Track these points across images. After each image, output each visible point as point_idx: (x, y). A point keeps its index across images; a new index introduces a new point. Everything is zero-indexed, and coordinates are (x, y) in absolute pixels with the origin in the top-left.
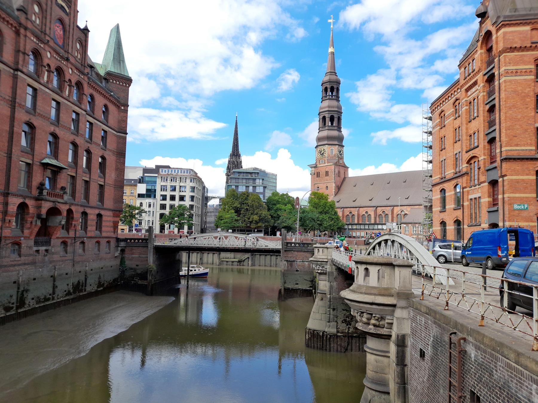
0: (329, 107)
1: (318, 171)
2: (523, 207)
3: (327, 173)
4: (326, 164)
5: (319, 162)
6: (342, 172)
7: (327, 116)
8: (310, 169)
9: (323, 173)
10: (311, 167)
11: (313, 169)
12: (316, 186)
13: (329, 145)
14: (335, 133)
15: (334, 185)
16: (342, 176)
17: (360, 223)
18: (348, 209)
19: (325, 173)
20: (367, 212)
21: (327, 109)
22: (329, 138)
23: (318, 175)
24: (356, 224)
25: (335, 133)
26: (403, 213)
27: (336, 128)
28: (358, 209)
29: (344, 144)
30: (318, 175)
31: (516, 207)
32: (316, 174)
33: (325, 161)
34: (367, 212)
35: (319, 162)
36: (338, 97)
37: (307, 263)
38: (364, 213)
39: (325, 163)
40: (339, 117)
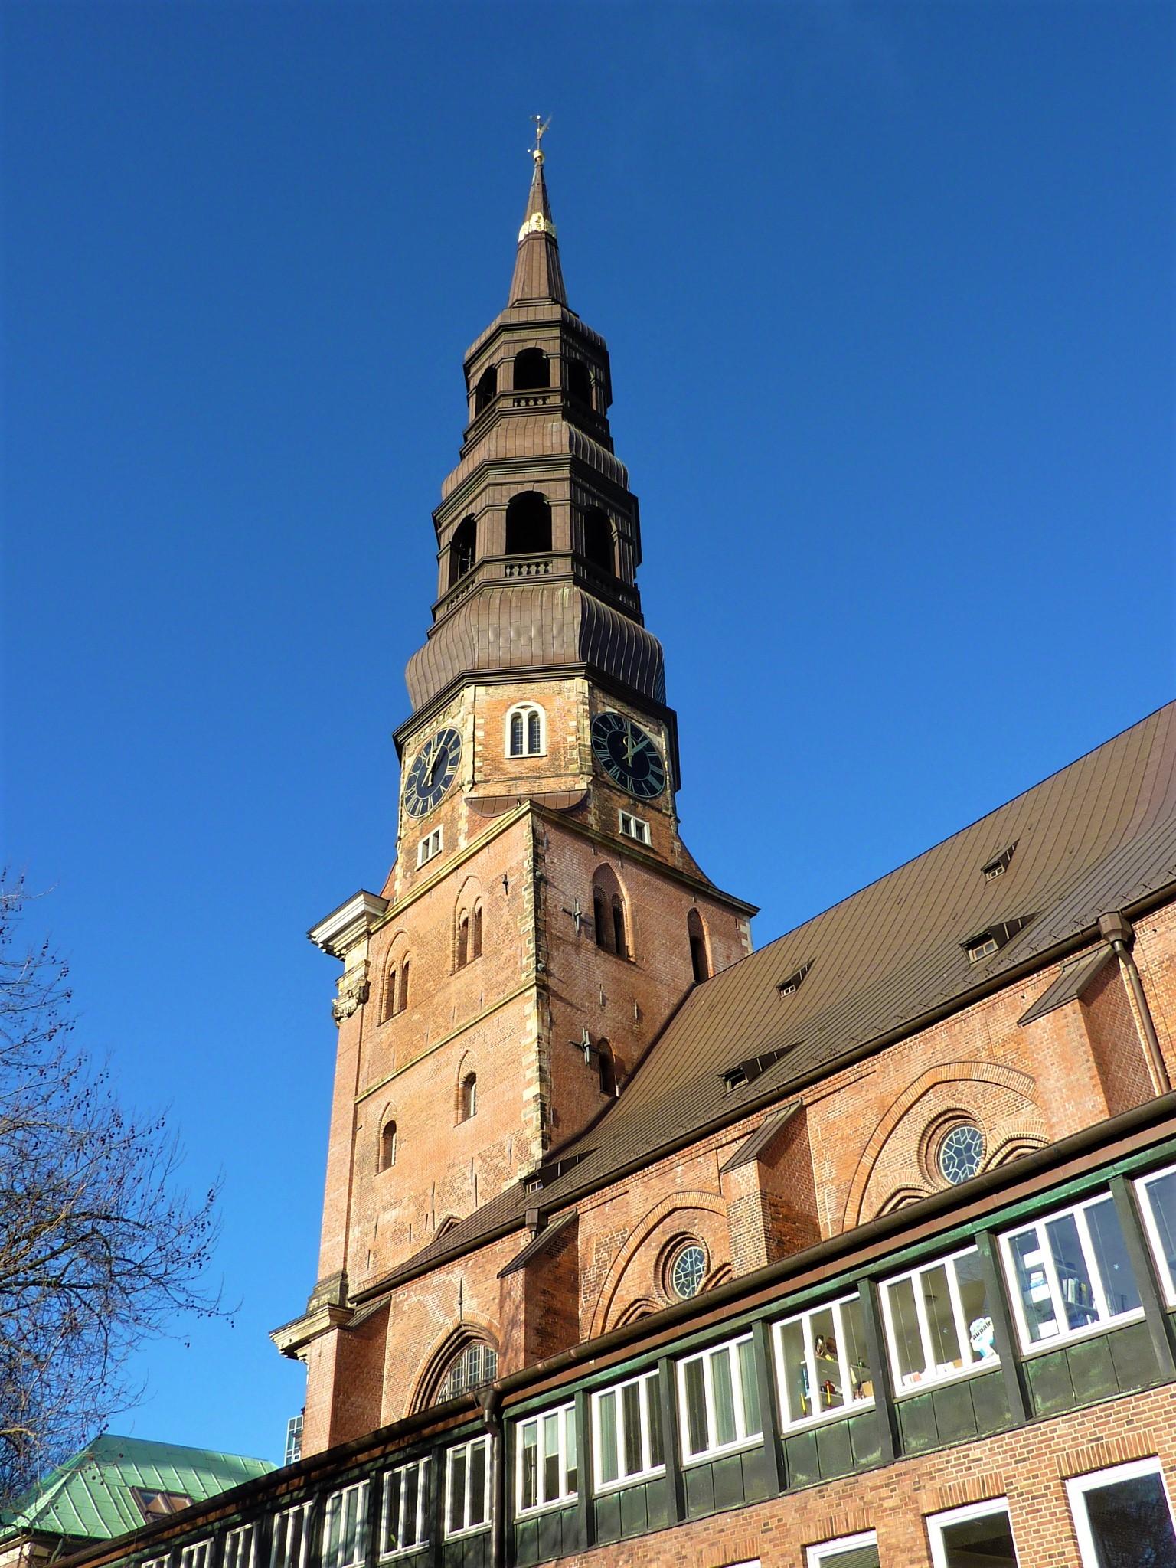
15: (533, 1025)
19: (451, 946)
32: (376, 994)
39: (452, 844)
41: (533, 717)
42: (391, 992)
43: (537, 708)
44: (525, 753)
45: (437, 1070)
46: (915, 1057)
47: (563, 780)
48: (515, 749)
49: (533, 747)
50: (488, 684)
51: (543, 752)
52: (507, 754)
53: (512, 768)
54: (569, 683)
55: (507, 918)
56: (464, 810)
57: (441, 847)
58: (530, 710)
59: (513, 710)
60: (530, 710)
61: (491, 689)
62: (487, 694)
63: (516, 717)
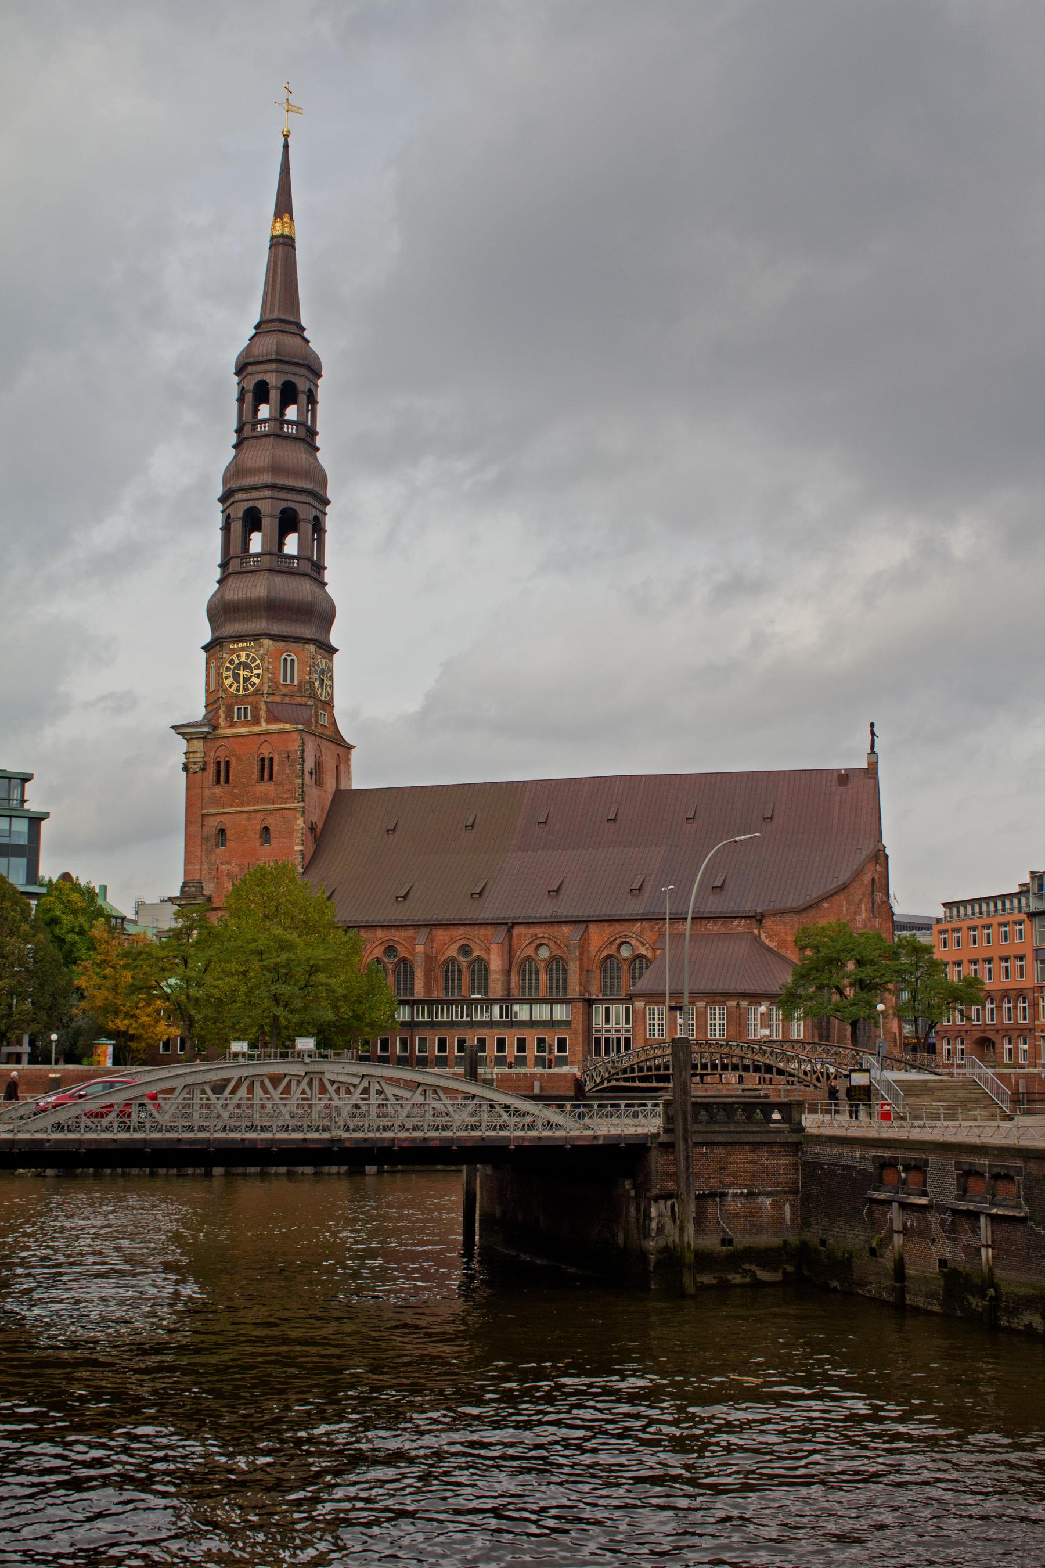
0: (275, 469)
1: (222, 755)
3: (266, 769)
4: (264, 726)
5: (229, 715)
6: (329, 763)
7: (265, 508)
8: (182, 745)
9: (244, 769)
10: (188, 737)
11: (198, 745)
12: (213, 823)
13: (276, 638)
14: (303, 589)
15: (300, 822)
16: (330, 785)
17: (436, 995)
18: (380, 934)
19: (256, 769)
20: (465, 950)
21: (266, 479)
22: (274, 608)
23: (223, 773)
24: (430, 1003)
25: (303, 589)
26: (625, 953)
27: (307, 568)
28: (424, 931)
29: (335, 638)
30: (223, 773)
32: (212, 769)
33: (256, 709)
34: (465, 950)
35: (229, 715)
36: (312, 433)
37: (768, 1201)
38: (453, 951)
39: (256, 721)
40: (316, 519)
41: (292, 660)
42: (218, 772)
45: (249, 819)
46: (461, 930)
48: (285, 680)
49: (292, 680)
51: (296, 683)
53: (284, 690)
54: (307, 646)
55: (287, 771)
56: (264, 707)
57: (249, 718)
59: (284, 656)
63: (285, 659)
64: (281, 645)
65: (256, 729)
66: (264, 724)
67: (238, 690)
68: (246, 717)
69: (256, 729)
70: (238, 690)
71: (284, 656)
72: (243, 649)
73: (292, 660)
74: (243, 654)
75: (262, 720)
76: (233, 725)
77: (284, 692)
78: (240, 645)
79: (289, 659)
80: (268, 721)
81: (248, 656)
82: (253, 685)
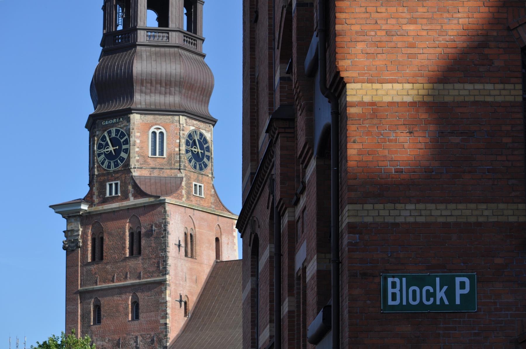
2: (441, 294)
31: (398, 291)
39: (125, 197)
43: (163, 130)
44: (157, 156)
47: (173, 171)
48: (154, 153)
49: (162, 153)
50: (141, 114)
51: (165, 156)
52: (150, 155)
53: (152, 164)
58: (160, 131)
59: (152, 129)
60: (160, 131)
61: (143, 116)
62: (141, 119)
63: (154, 133)
64: (149, 118)
65: (125, 203)
66: (132, 198)
67: (109, 167)
68: (116, 193)
69: (125, 203)
70: (109, 167)
71: (152, 129)
72: (113, 125)
73: (161, 133)
74: (113, 130)
75: (130, 195)
76: (105, 201)
77: (152, 165)
78: (111, 122)
79: (158, 132)
80: (135, 196)
81: (117, 131)
82: (122, 159)
